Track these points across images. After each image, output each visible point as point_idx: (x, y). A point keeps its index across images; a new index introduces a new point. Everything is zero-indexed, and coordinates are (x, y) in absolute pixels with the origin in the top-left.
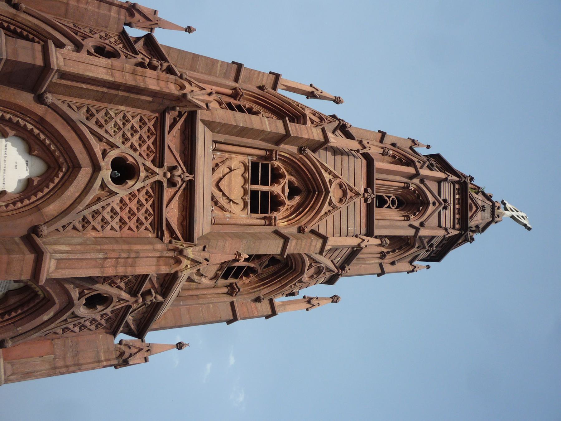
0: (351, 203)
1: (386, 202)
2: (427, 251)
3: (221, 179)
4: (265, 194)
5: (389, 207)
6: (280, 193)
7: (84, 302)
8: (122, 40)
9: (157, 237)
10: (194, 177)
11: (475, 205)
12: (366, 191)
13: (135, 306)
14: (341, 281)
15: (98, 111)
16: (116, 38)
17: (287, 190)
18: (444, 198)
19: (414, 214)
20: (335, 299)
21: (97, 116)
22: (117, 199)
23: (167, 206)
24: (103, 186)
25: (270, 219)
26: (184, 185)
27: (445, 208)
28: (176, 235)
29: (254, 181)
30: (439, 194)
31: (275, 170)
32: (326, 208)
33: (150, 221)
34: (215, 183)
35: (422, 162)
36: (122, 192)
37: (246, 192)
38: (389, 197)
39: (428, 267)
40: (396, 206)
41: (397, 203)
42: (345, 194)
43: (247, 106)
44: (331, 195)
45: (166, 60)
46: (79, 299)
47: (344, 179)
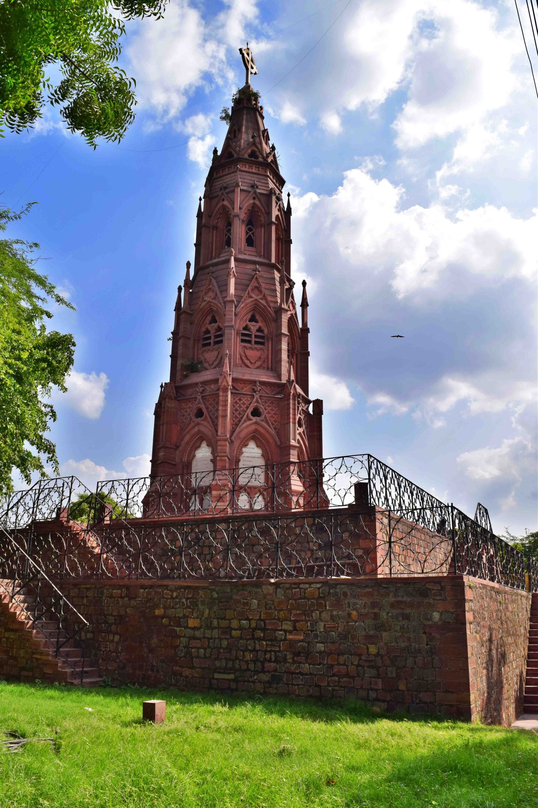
5: (253, 234)
14: (293, 277)
16: (183, 404)
17: (254, 323)
20: (304, 283)
22: (267, 415)
24: (262, 421)
27: (257, 187)
30: (250, 192)
32: (263, 302)
35: (223, 197)
36: (264, 413)
37: (256, 349)
38: (247, 233)
39: (289, 195)
42: (256, 287)
44: (257, 298)
45: (197, 384)
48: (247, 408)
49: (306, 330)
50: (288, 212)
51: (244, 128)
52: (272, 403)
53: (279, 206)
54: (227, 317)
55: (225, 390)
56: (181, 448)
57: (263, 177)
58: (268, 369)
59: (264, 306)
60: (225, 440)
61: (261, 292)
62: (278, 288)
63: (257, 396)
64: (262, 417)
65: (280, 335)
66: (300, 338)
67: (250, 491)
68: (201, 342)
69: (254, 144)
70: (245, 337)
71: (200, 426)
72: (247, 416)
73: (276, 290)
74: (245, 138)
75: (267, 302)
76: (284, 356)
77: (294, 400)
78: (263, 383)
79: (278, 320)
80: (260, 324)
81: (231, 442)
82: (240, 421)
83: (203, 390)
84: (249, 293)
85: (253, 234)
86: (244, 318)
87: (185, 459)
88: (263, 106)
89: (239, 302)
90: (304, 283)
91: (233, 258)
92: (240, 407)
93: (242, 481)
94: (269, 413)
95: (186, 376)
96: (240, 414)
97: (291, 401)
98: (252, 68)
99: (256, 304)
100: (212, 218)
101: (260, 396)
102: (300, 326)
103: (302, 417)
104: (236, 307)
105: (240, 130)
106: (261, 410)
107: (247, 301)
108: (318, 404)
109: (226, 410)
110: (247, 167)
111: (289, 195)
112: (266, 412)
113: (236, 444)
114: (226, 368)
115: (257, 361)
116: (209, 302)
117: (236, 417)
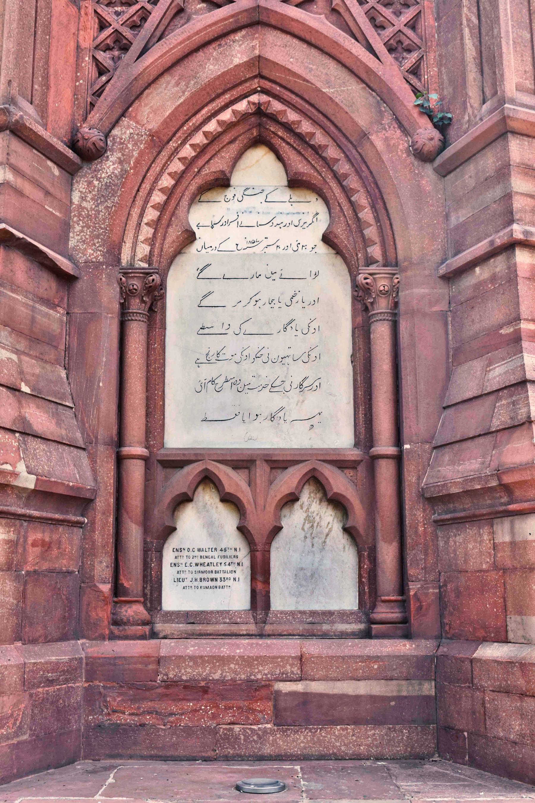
15: (103, 25)
67: (255, 485)
82: (145, 15)
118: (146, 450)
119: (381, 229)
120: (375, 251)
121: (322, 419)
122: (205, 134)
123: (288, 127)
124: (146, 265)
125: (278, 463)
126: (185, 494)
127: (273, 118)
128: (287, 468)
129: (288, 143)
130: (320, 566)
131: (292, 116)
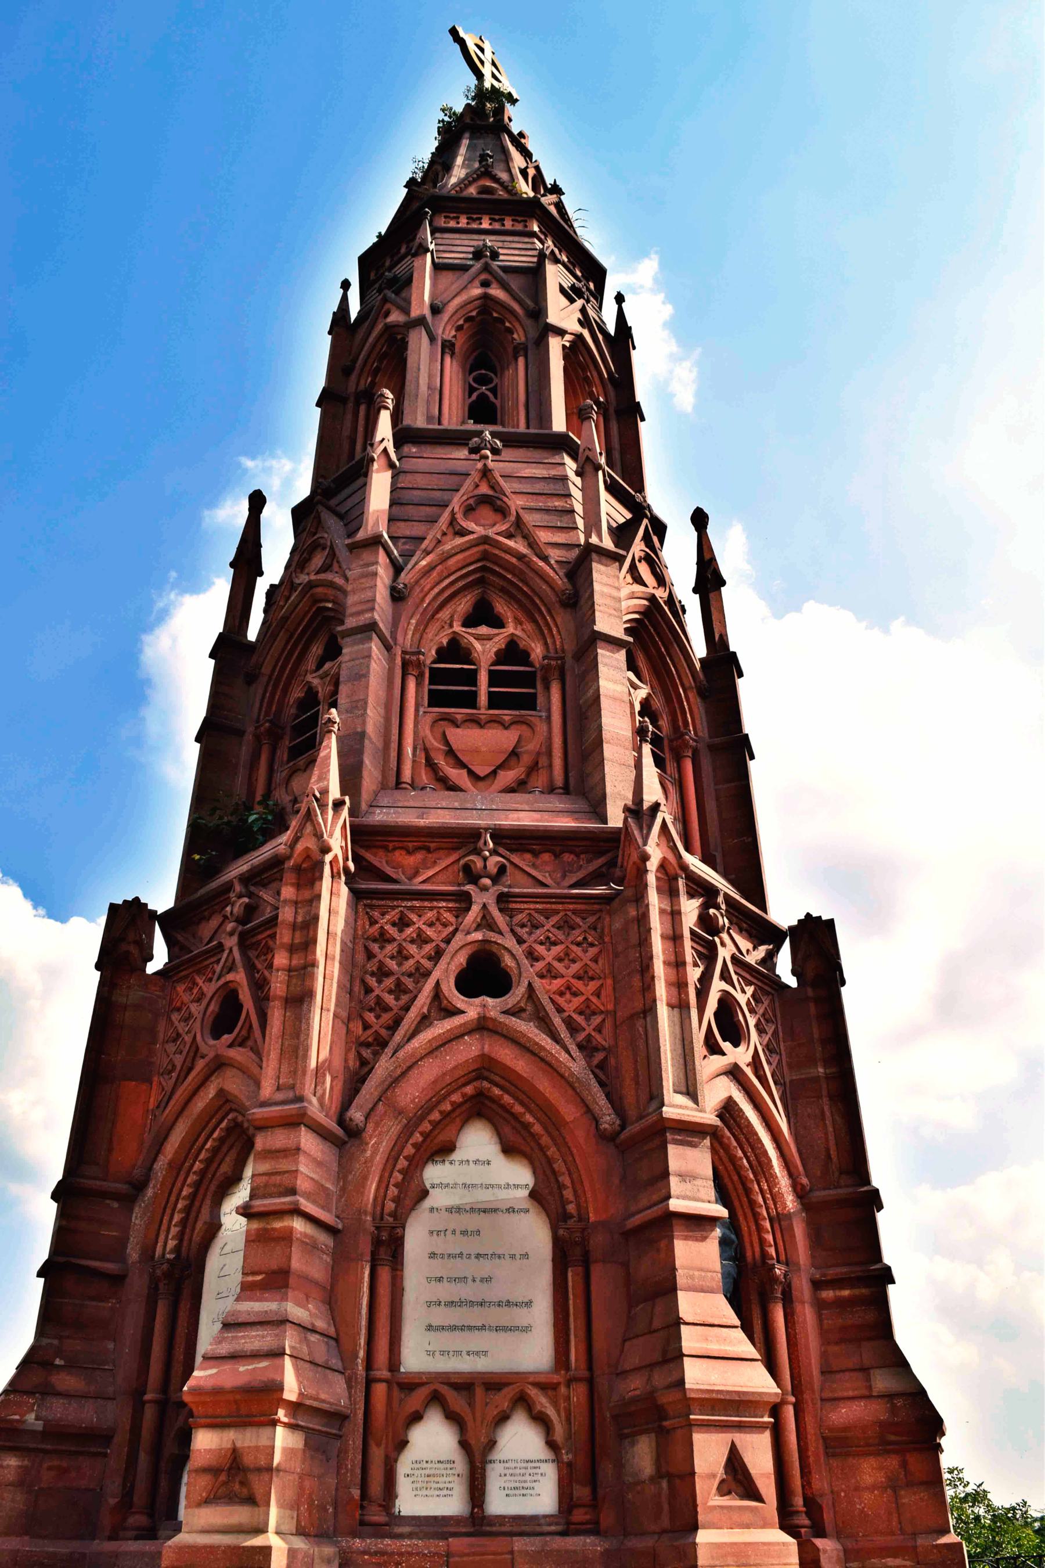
0: (506, 486)
1: (482, 396)
2: (588, 301)
3: (471, 773)
4: (495, 678)
5: (494, 391)
6: (489, 644)
7: (728, 1043)
8: (186, 977)
9: (608, 904)
10: (486, 829)
11: (479, 177)
12: (475, 450)
13: (735, 950)
16: (181, 988)
17: (483, 630)
18: (471, 256)
19: (510, 331)
21: (376, 1028)
23: (543, 885)
24: (515, 1012)
25: (546, 669)
26: (501, 850)
27: (495, 255)
28: (600, 867)
29: (469, 700)
30: (464, 268)
31: (443, 654)
33: (578, 920)
34: (481, 784)
35: (388, 306)
36: (526, 974)
38: (472, 390)
39: (620, 299)
40: (493, 375)
41: (483, 372)
42: (484, 500)
43: (293, 711)
44: (491, 533)
45: (228, 887)
46: (723, 1054)
47: (456, 503)
48: (437, 956)
49: (723, 664)
50: (622, 339)
51: (459, 160)
52: (566, 925)
53: (583, 311)
54: (351, 600)
55: (309, 873)
56: (150, 1192)
57: (516, 239)
58: (551, 790)
59: (521, 557)
60: (296, 1121)
61: (502, 511)
62: (579, 508)
63: (483, 899)
64: (516, 996)
65: (591, 641)
66: (702, 693)
67: (475, 1404)
68: (286, 743)
69: (486, 172)
70: (449, 684)
71: (230, 1072)
72: (437, 994)
73: (573, 511)
74: (458, 173)
75: (532, 544)
76: (616, 723)
77: (669, 891)
78: (513, 840)
79: (577, 596)
80: (511, 629)
81: (345, 1137)
82: (397, 1022)
83: (250, 911)
84: (453, 521)
85: (494, 391)
86: (445, 614)
87: (167, 1245)
88: (526, 132)
89: (408, 555)
90: (700, 519)
91: (385, 420)
92: (402, 955)
93: (418, 1355)
94: (549, 973)
95: (212, 870)
96: (399, 989)
97: (653, 898)
98: (494, 76)
99: (485, 556)
100: (354, 377)
101: (502, 899)
102: (699, 648)
103: (742, 999)
104: (397, 569)
105: (448, 168)
106: (508, 961)
107: (447, 547)
108: (816, 939)
109: (304, 971)
110: (466, 221)
111: (620, 299)
112: (530, 972)
113: (377, 1145)
114: (324, 776)
115: (502, 766)
116: (311, 585)
117: (381, 1006)
118: (389, 1374)
119: (575, 1191)
120: (571, 1208)
121: (530, 1349)
122: (441, 1112)
123: (503, 1107)
124: (391, 1219)
125: (494, 1383)
126: (417, 1412)
127: (492, 1099)
128: (499, 1390)
129: (504, 1119)
130: (526, 1475)
131: (507, 1099)
